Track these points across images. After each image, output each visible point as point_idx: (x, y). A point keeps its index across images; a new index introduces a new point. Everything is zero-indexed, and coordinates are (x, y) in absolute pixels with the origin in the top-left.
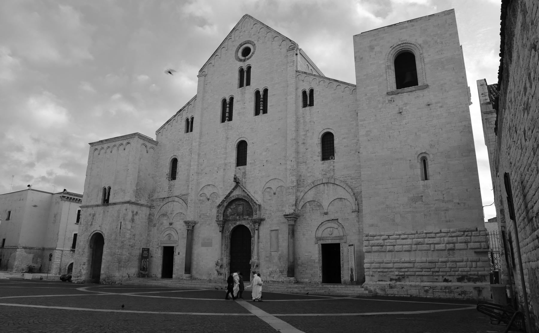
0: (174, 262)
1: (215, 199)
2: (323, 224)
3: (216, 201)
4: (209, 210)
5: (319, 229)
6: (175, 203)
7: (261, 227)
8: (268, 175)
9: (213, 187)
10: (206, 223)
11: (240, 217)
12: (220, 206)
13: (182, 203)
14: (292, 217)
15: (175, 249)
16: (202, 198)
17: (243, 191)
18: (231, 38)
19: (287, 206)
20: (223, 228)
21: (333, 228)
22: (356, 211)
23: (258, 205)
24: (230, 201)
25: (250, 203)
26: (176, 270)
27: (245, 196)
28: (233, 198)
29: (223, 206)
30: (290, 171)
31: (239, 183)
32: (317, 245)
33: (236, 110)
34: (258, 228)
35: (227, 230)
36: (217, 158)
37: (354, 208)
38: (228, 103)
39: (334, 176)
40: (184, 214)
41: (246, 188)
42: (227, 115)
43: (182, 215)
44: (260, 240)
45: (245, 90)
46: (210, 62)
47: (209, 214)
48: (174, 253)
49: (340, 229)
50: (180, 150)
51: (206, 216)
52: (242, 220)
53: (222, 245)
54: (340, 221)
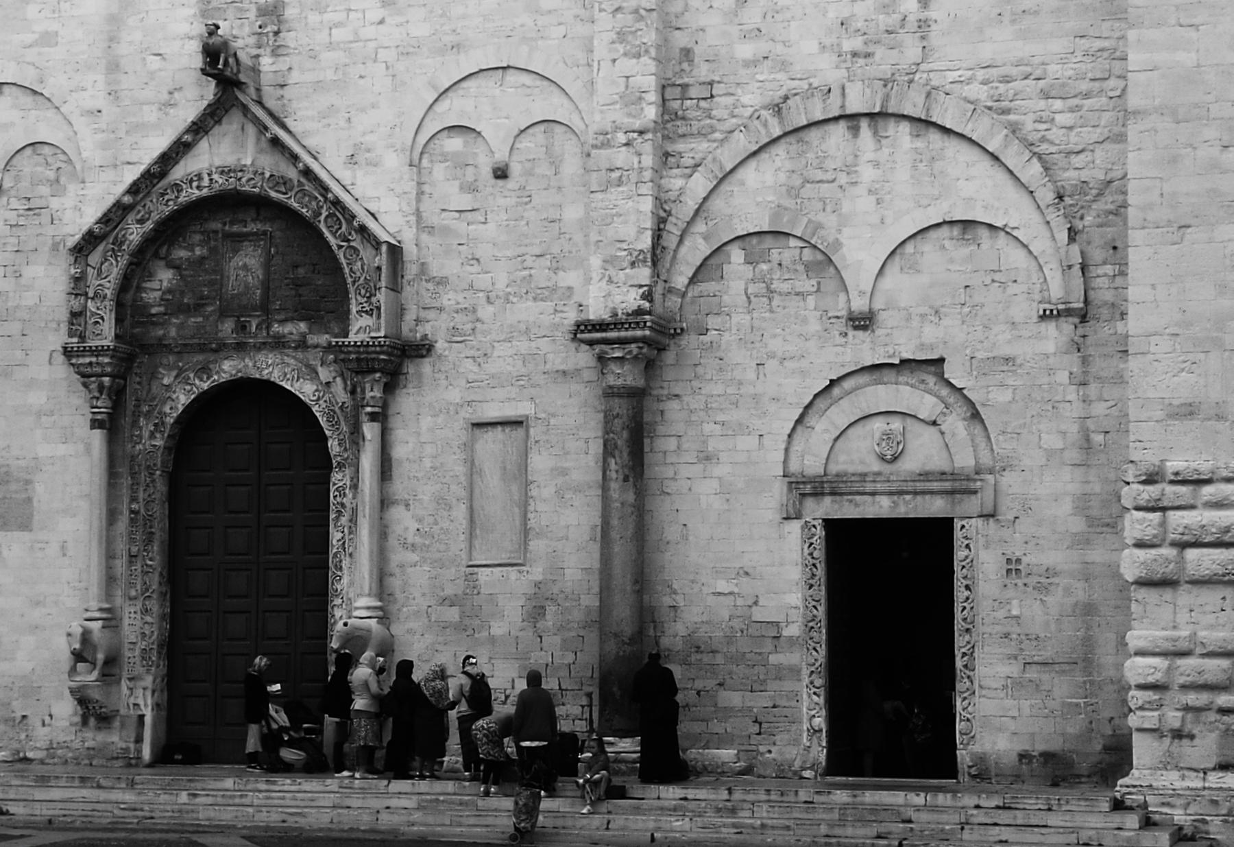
1: (44, 190)
2: (836, 391)
3: (55, 203)
5: (811, 420)
7: (406, 403)
8: (449, 39)
11: (242, 328)
12: (90, 240)
14: (634, 340)
17: (264, 144)
19: (596, 262)
20: (117, 396)
21: (909, 421)
22: (1069, 312)
23: (384, 248)
24: (167, 211)
25: (325, 230)
27: (285, 182)
28: (192, 193)
29: (119, 243)
30: (619, 16)
31: (239, 84)
32: (795, 527)
34: (385, 406)
35: (148, 415)
37: (1056, 290)
39: (923, 67)
41: (289, 122)
44: (399, 487)
49: (956, 424)
52: (260, 347)
53: (112, 516)
54: (955, 373)
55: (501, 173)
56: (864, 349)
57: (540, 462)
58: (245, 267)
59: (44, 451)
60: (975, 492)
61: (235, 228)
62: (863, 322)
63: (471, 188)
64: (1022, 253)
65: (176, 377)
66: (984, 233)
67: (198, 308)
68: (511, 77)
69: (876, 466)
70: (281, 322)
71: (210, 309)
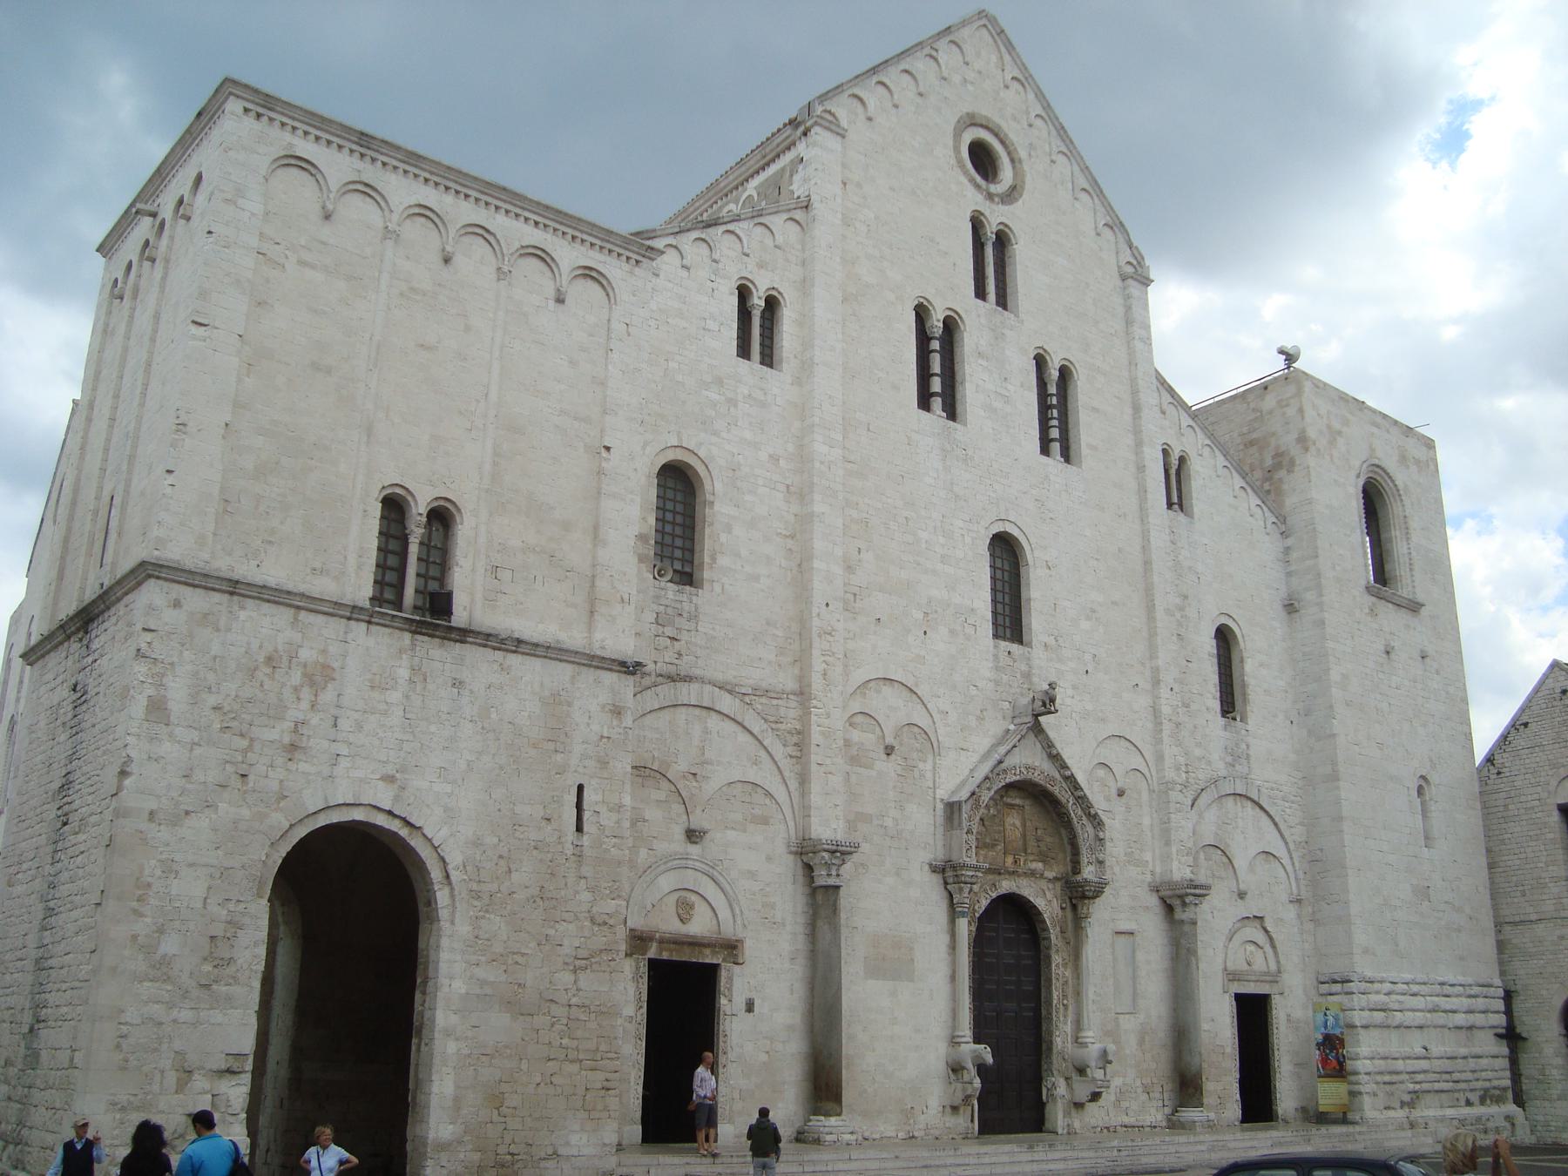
1: (915, 755)
3: (921, 765)
4: (893, 805)
6: (713, 721)
9: (906, 693)
15: (730, 979)
16: (856, 735)
18: (936, 60)
33: (977, 386)
36: (919, 564)
38: (937, 335)
40: (768, 794)
42: (936, 385)
46: (856, 91)
48: (723, 1001)
50: (715, 433)
55: (1121, 793)
56: (1243, 909)
57: (1140, 956)
58: (1014, 825)
60: (1277, 982)
61: (1009, 800)
62: (1242, 895)
63: (1108, 799)
64: (1282, 870)
65: (981, 887)
66: (1272, 858)
67: (994, 846)
68: (1123, 742)
69: (1246, 967)
70: (1031, 861)
71: (999, 847)
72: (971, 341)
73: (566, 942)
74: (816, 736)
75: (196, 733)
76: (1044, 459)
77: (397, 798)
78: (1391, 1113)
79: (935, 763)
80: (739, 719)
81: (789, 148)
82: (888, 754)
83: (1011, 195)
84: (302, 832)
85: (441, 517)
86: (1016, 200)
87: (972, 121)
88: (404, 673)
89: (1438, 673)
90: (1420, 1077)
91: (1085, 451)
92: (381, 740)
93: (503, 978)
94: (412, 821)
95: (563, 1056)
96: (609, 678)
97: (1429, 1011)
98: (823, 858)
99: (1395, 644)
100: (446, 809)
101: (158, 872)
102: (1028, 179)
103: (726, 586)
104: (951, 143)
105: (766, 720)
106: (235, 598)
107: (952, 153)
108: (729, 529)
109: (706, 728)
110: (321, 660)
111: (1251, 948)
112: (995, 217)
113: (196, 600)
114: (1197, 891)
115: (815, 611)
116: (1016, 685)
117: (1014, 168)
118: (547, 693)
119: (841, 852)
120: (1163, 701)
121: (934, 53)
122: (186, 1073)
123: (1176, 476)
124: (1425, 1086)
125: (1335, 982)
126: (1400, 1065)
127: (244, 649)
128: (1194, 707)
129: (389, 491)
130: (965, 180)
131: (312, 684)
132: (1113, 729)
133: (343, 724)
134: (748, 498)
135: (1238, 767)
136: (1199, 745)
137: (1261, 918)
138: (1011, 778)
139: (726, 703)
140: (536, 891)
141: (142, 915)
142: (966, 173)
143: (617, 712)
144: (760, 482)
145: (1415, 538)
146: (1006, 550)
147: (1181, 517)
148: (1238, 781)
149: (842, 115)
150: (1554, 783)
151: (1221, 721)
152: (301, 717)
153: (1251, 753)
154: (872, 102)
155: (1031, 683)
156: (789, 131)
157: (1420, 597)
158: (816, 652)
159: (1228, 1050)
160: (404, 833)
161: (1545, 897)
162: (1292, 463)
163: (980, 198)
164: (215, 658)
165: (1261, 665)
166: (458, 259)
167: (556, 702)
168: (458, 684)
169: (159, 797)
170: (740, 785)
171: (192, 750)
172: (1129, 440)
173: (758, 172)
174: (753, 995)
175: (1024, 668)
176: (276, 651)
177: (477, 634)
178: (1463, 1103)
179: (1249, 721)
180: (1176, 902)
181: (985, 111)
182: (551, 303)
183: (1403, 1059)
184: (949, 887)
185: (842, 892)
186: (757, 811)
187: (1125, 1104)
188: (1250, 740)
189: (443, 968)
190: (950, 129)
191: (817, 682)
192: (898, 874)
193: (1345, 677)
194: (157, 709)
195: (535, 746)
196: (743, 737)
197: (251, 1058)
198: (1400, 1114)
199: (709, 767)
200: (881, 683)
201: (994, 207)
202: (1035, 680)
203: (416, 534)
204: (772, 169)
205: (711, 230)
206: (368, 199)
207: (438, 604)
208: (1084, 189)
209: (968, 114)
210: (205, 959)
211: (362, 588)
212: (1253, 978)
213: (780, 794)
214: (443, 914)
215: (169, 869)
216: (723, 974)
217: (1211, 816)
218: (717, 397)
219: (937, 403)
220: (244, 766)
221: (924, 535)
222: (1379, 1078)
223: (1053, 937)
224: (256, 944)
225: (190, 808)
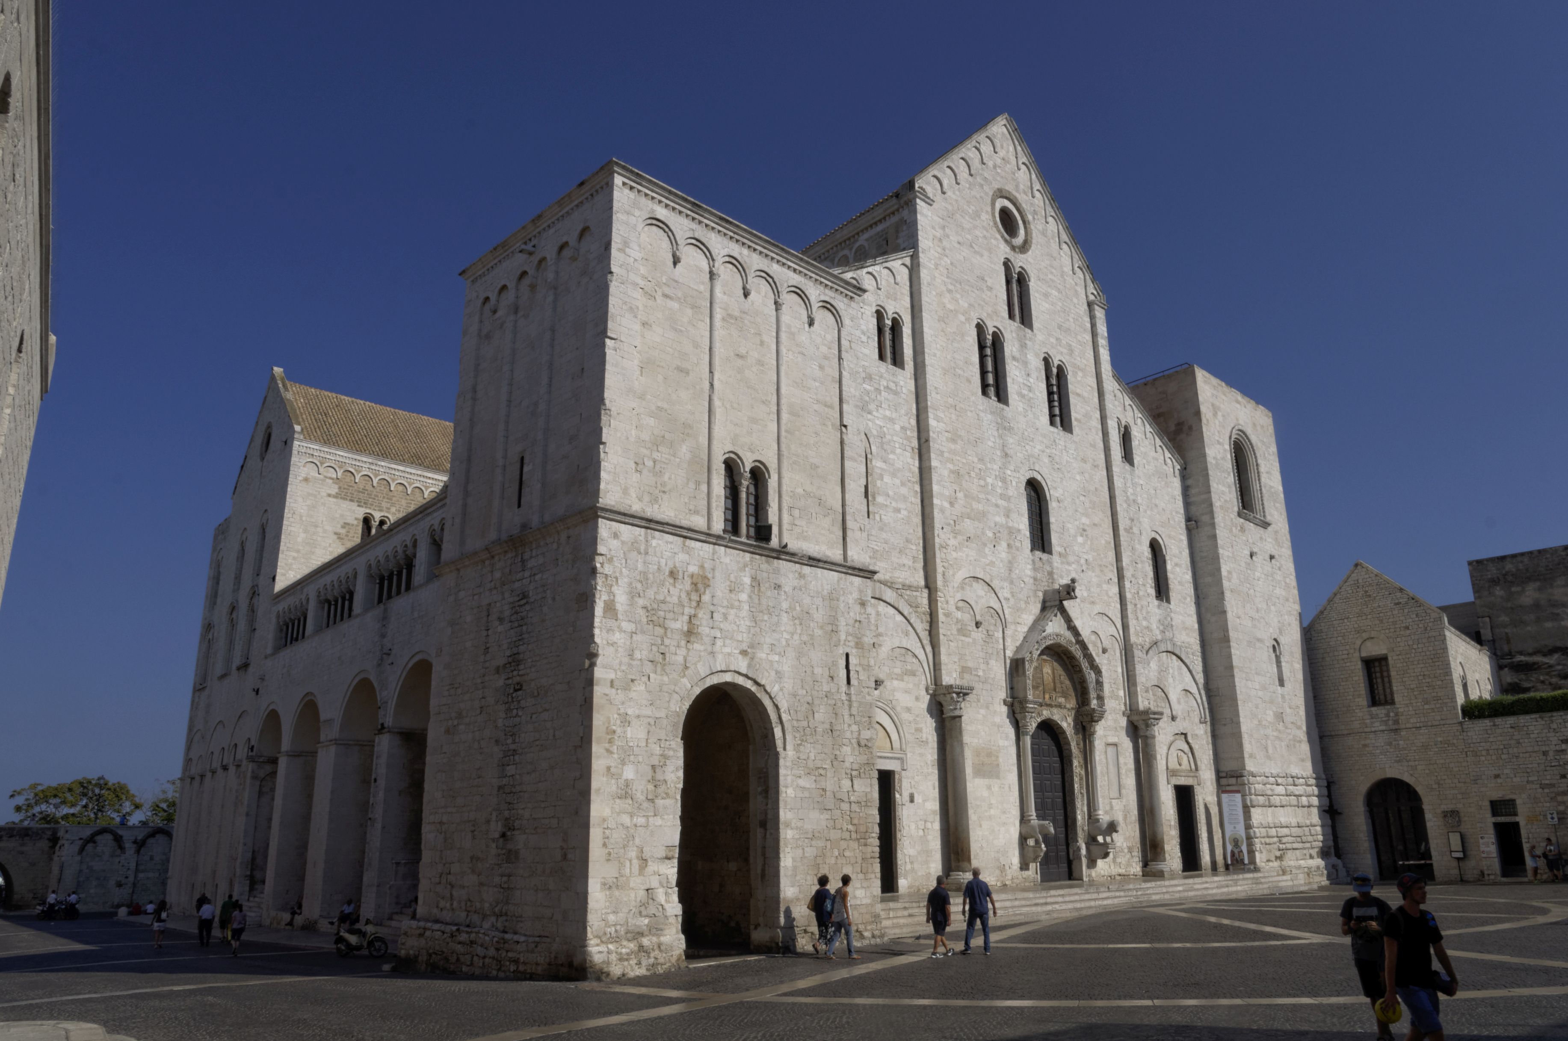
0: (900, 831)
1: (992, 628)
4: (982, 661)
6: (882, 607)
9: (986, 587)
10: (979, 701)
13: (910, 613)
15: (900, 780)
16: (959, 615)
26: (908, 860)
42: (991, 379)
43: (910, 658)
45: (1025, 336)
47: (984, 670)
48: (897, 796)
50: (870, 413)
51: (977, 679)
55: (1104, 651)
57: (1122, 760)
58: (1048, 673)
59: (1002, 743)
69: (1178, 767)
72: (1010, 348)
73: (846, 760)
74: (941, 618)
75: (634, 625)
76: (1052, 429)
77: (749, 666)
78: (1271, 864)
79: (1003, 632)
80: (896, 606)
81: (893, 213)
82: (977, 627)
83: (1024, 247)
84: (697, 691)
85: (758, 475)
86: (1028, 250)
87: (1001, 194)
88: (747, 580)
89: (1280, 569)
90: (1284, 840)
91: (1074, 423)
92: (738, 626)
93: (813, 786)
94: (759, 681)
95: (848, 837)
96: (857, 581)
97: (1287, 795)
98: (952, 698)
99: (1255, 550)
100: (777, 672)
101: (618, 722)
102: (1034, 235)
103: (883, 517)
104: (989, 209)
105: (911, 606)
106: (649, 531)
107: (990, 217)
108: (881, 477)
109: (878, 612)
110: (701, 573)
111: (1180, 753)
112: (1019, 261)
113: (627, 531)
114: (1156, 716)
115: (936, 532)
116: (1044, 580)
117: (1025, 228)
118: (825, 592)
119: (964, 693)
120: (1127, 590)
121: (978, 145)
122: (644, 862)
123: (1126, 437)
124: (1289, 846)
125: (1233, 777)
126: (1273, 832)
127: (656, 567)
128: (1141, 593)
129: (727, 456)
130: (999, 237)
131: (697, 591)
132: (1098, 608)
133: (715, 615)
134: (891, 456)
135: (1167, 633)
136: (1145, 618)
137: (1185, 735)
138: (1049, 643)
139: (889, 595)
140: (827, 726)
141: (611, 753)
142: (999, 231)
143: (863, 604)
144: (897, 445)
145: (1263, 480)
146: (1035, 489)
147: (1127, 467)
148: (1168, 643)
149: (929, 191)
150: (1359, 642)
151: (1156, 602)
152: (693, 612)
153: (1174, 623)
154: (945, 183)
155: (1053, 579)
156: (894, 200)
157: (1269, 518)
158: (938, 561)
159: (1173, 823)
160: (754, 689)
161: (1353, 719)
162: (1190, 428)
163: (1008, 249)
164: (641, 572)
165: (1176, 565)
166: (753, 296)
167: (832, 598)
168: (778, 587)
169: (615, 670)
170: (898, 650)
171: (632, 637)
172: (1098, 415)
173: (866, 229)
174: (913, 791)
175: (1049, 569)
176: (675, 567)
177: (787, 553)
178: (1308, 857)
179: (1172, 602)
180: (1142, 726)
181: (1010, 188)
182: (807, 326)
183: (1275, 827)
184: (1016, 715)
185: (963, 718)
186: (909, 667)
187: (1119, 860)
188: (1172, 615)
189: (781, 778)
190: (989, 200)
191: (939, 578)
192: (987, 708)
193: (1229, 572)
194: (610, 608)
195: (822, 628)
196: (899, 618)
197: (677, 850)
198: (1276, 864)
199: (881, 638)
200: (971, 579)
201: (1016, 255)
202: (1055, 576)
203: (745, 483)
204: (880, 228)
205: (858, 272)
206: (699, 251)
207: (762, 533)
208: (1066, 243)
209: (998, 189)
210: (649, 781)
211: (719, 525)
212: (1184, 774)
213: (922, 656)
214: (779, 743)
215: (625, 720)
216: (897, 776)
217: (1153, 665)
218: (868, 387)
219: (992, 391)
220: (663, 647)
221: (989, 480)
222: (1263, 840)
223: (1073, 748)
224: (677, 770)
225: (633, 677)
